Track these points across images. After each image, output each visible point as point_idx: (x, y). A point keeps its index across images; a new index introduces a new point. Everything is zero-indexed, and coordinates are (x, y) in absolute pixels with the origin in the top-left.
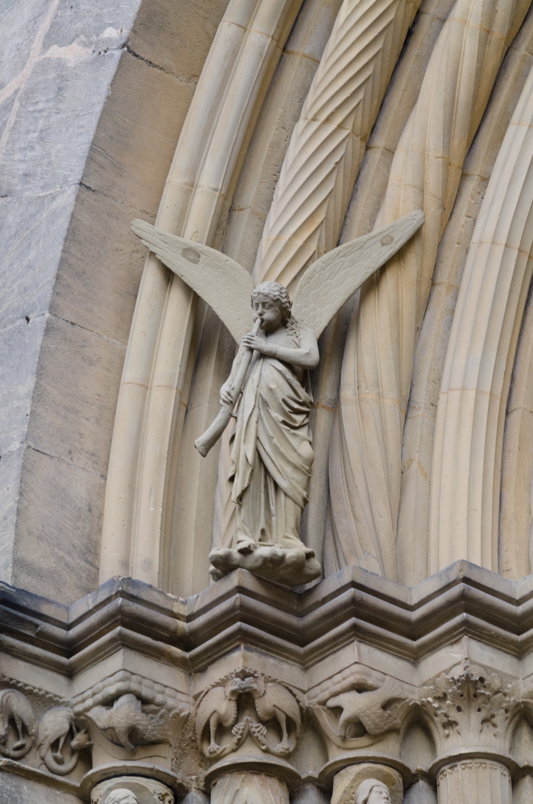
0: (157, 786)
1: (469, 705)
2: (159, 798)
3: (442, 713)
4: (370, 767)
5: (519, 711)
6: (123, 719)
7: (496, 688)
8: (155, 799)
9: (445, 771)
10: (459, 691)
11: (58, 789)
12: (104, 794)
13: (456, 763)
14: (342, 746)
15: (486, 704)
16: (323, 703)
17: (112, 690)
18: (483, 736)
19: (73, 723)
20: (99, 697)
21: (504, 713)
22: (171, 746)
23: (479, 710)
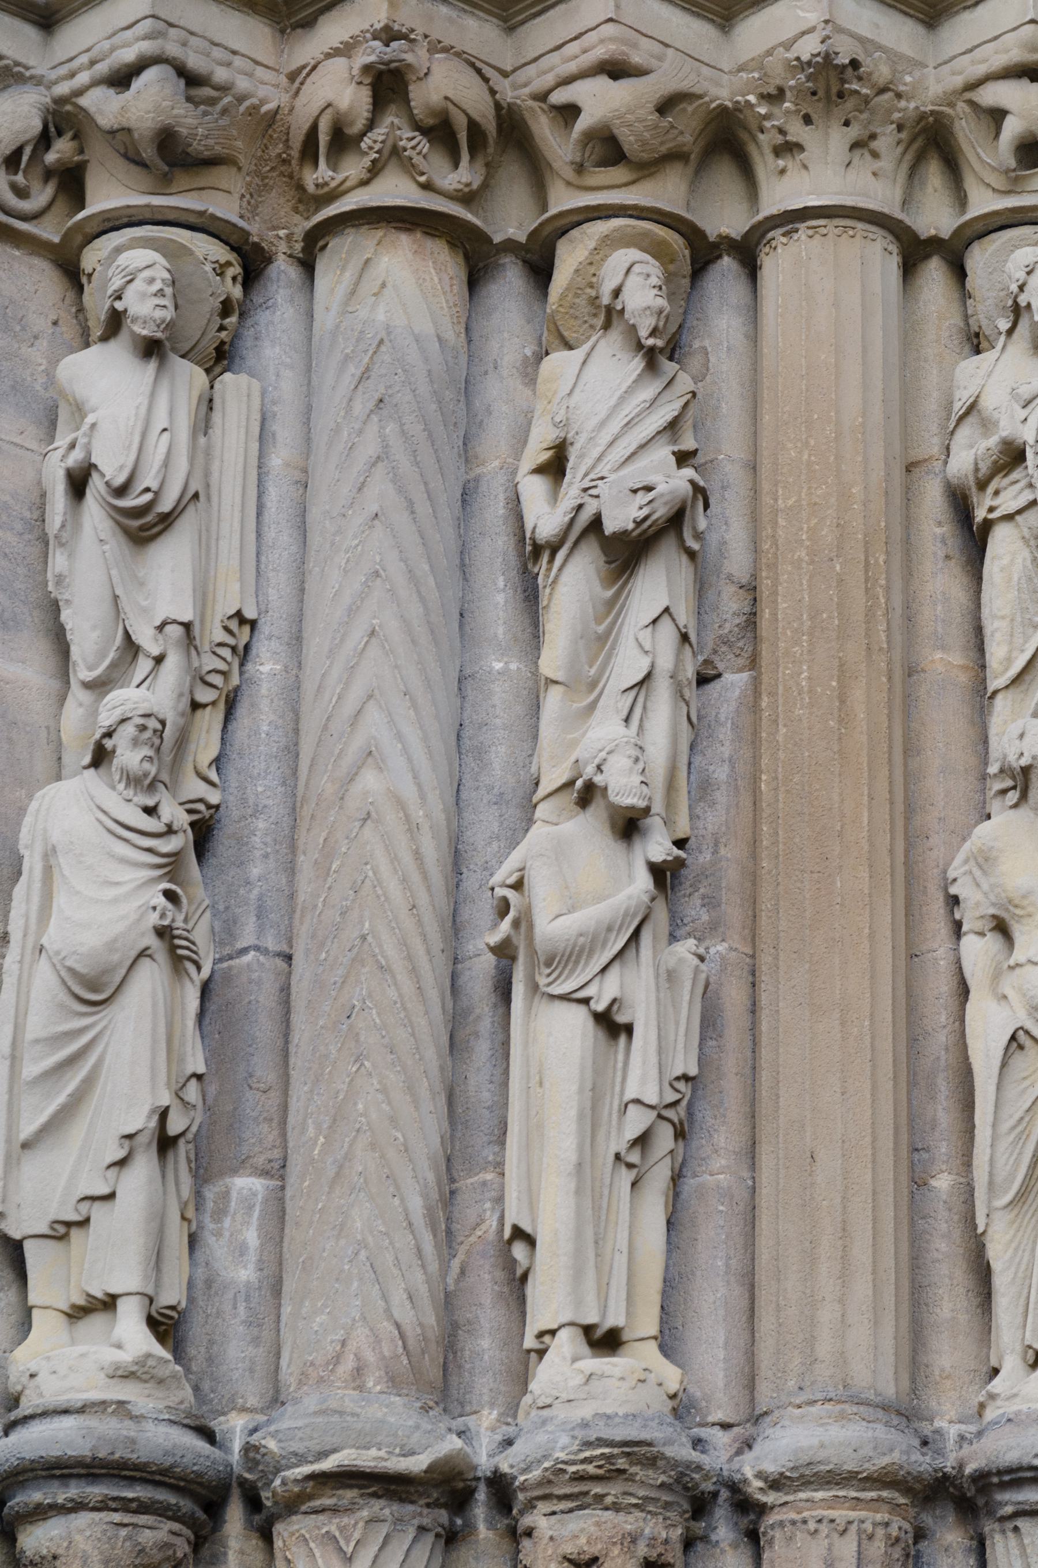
0: (211, 247)
1: (828, 112)
2: (214, 269)
3: (773, 126)
4: (629, 226)
5: (923, 130)
6: (149, 112)
7: (881, 82)
8: (206, 272)
10: (810, 84)
11: (18, 247)
12: (108, 258)
13: (797, 225)
14: (575, 183)
15: (861, 112)
16: (542, 97)
17: (129, 55)
19: (50, 118)
20: (102, 68)
21: (895, 132)
22: (240, 169)
23: (847, 124)
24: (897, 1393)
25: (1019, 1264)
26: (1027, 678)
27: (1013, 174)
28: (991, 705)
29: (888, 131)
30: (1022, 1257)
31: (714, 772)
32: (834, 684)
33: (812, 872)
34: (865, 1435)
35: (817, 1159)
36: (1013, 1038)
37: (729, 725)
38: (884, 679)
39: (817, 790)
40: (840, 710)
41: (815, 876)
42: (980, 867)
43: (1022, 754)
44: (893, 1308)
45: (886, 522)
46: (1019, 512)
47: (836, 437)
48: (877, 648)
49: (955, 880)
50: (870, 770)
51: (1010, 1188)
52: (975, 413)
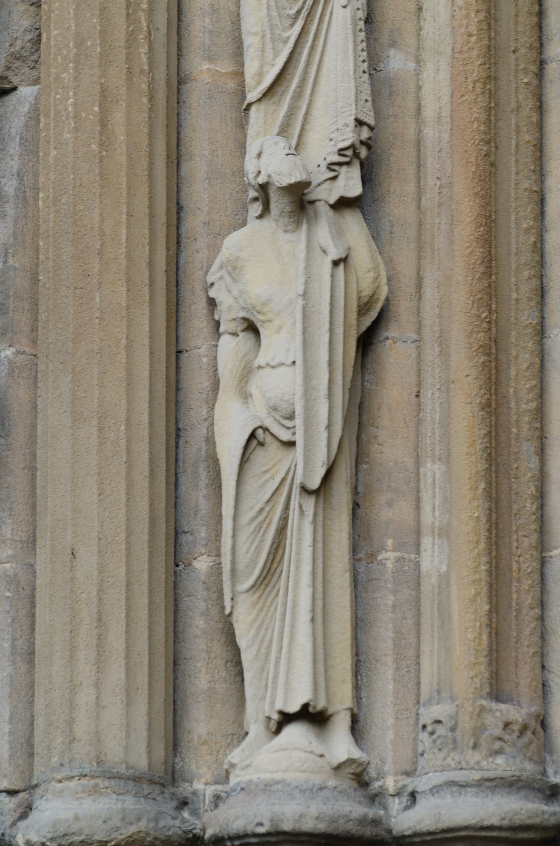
24: (150, 764)
25: (262, 641)
26: (279, 89)
30: (265, 635)
31: (5, 184)
32: (96, 109)
33: (75, 288)
34: (114, 807)
35: (77, 556)
36: (253, 436)
37: (18, 140)
38: (145, 100)
39: (80, 211)
40: (101, 134)
41: (78, 291)
42: (230, 274)
43: (260, 172)
44: (146, 686)
48: (138, 70)
49: (212, 284)
50: (129, 189)
51: (252, 573)
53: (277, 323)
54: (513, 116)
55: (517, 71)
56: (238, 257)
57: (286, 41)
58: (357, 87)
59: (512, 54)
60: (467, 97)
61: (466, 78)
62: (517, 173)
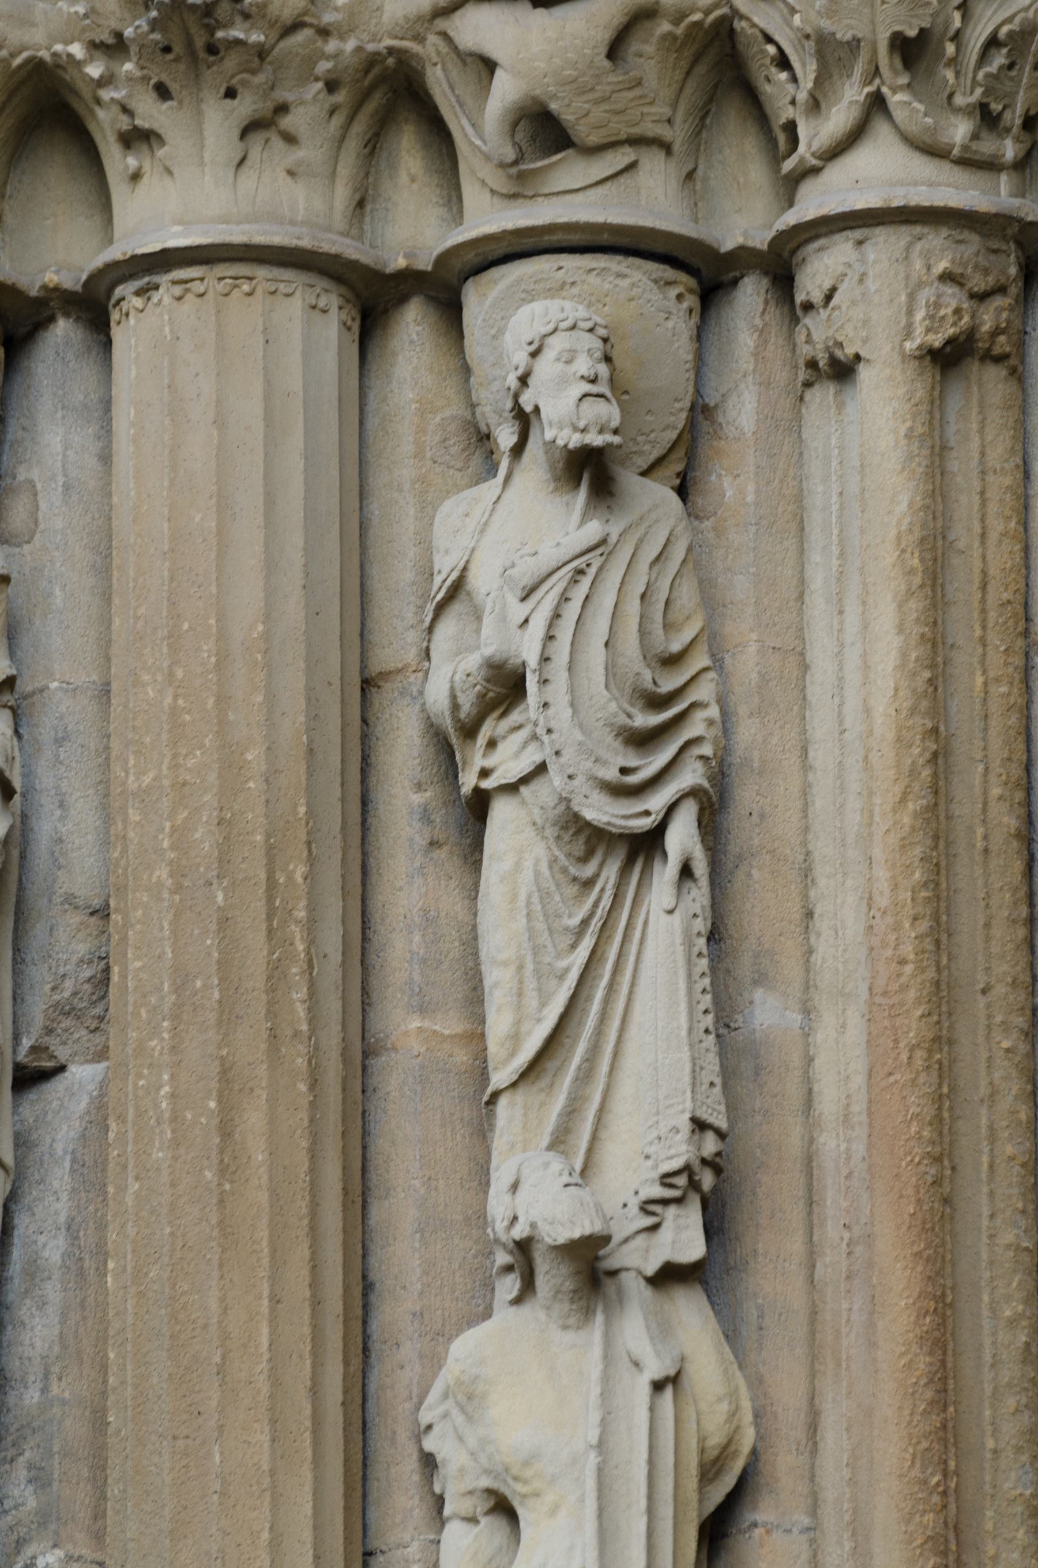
1: (196, 76)
3: (112, 99)
5: (383, 79)
7: (287, 15)
9: (123, 299)
10: (156, 36)
13: (155, 279)
15: (254, 72)
18: (248, 179)
21: (323, 95)
23: (231, 94)
26: (551, 1065)
27: (513, 171)
28: (491, 1115)
29: (309, 96)
31: (44, 1246)
32: (212, 1104)
33: (175, 1438)
37: (67, 1164)
38: (303, 1087)
40: (222, 1151)
41: (181, 1443)
42: (462, 1409)
43: (515, 1218)
45: (308, 805)
46: (525, 780)
47: (218, 663)
48: (289, 1032)
49: (429, 1427)
50: (273, 1252)
52: (463, 596)
53: (549, 1498)
54: (984, 1111)
55: (989, 1027)
56: (477, 1377)
57: (562, 977)
58: (694, 1060)
59: (979, 996)
60: (897, 1076)
61: (896, 1041)
62: (992, 1216)
